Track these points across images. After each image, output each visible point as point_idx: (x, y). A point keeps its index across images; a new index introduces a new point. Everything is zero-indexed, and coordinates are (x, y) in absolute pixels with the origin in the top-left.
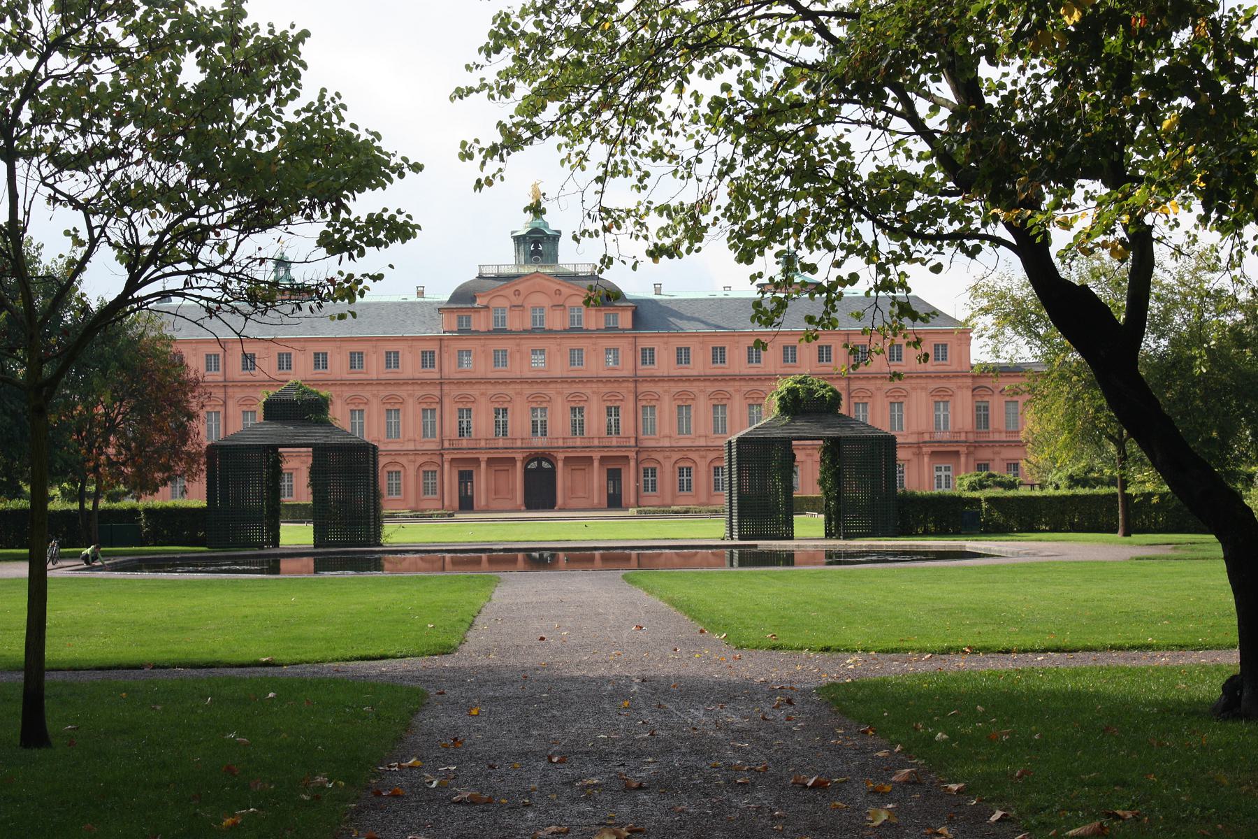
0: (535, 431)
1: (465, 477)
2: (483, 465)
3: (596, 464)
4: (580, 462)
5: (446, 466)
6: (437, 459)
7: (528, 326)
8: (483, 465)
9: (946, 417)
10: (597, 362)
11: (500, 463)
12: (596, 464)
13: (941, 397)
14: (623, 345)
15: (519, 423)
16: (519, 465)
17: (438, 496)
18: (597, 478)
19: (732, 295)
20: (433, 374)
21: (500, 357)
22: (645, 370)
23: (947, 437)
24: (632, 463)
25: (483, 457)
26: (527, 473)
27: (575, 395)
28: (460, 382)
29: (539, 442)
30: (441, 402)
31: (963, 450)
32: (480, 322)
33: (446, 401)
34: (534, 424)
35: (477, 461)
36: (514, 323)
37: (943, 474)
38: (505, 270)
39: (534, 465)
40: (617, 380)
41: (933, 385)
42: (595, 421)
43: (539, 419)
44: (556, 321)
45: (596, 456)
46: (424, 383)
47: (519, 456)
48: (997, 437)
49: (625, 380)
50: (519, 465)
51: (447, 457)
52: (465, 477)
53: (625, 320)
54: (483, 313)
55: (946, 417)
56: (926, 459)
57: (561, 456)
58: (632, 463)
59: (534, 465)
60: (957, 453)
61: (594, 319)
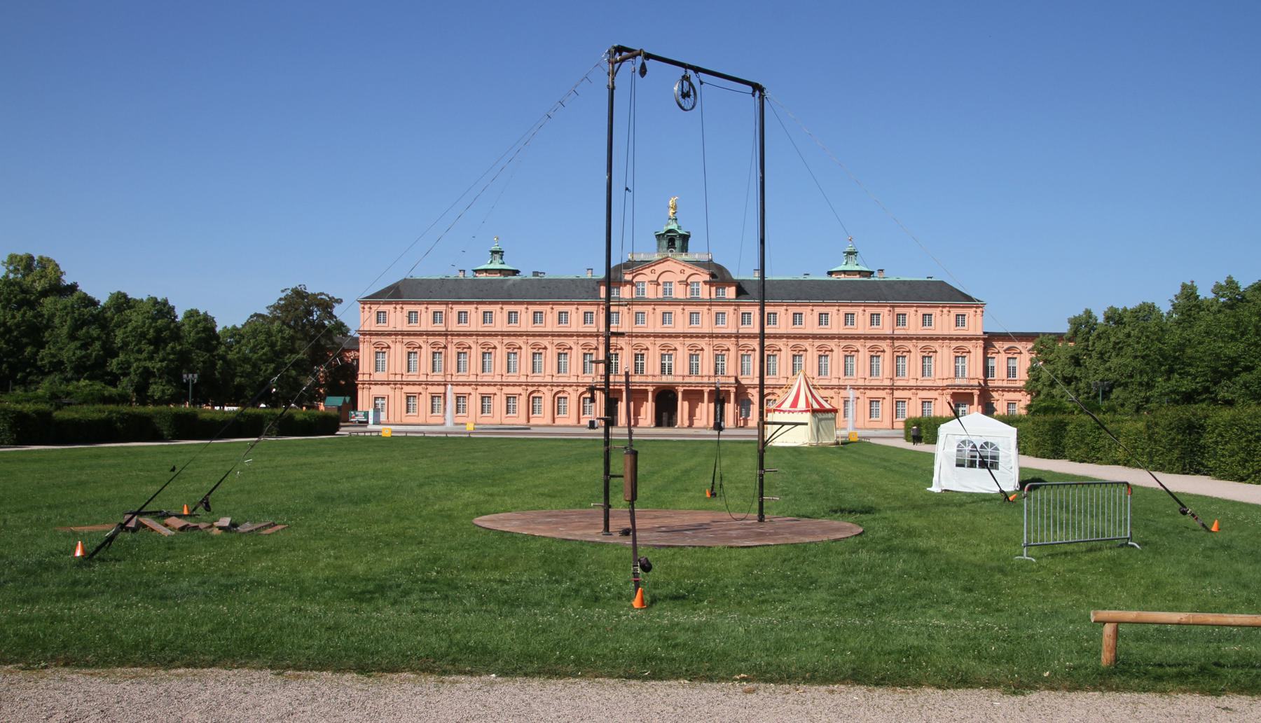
0: (663, 371)
4: (694, 396)
7: (660, 295)
9: (963, 367)
10: (706, 324)
13: (960, 354)
14: (730, 310)
15: (652, 365)
16: (650, 395)
19: (808, 278)
21: (638, 317)
23: (965, 382)
27: (693, 346)
29: (666, 379)
32: (625, 292)
34: (663, 365)
36: (650, 292)
40: (723, 336)
41: (955, 344)
42: (706, 364)
43: (667, 362)
44: (679, 292)
45: (706, 390)
46: (585, 335)
47: (650, 389)
49: (729, 336)
53: (730, 292)
54: (629, 286)
57: (680, 389)
61: (704, 292)
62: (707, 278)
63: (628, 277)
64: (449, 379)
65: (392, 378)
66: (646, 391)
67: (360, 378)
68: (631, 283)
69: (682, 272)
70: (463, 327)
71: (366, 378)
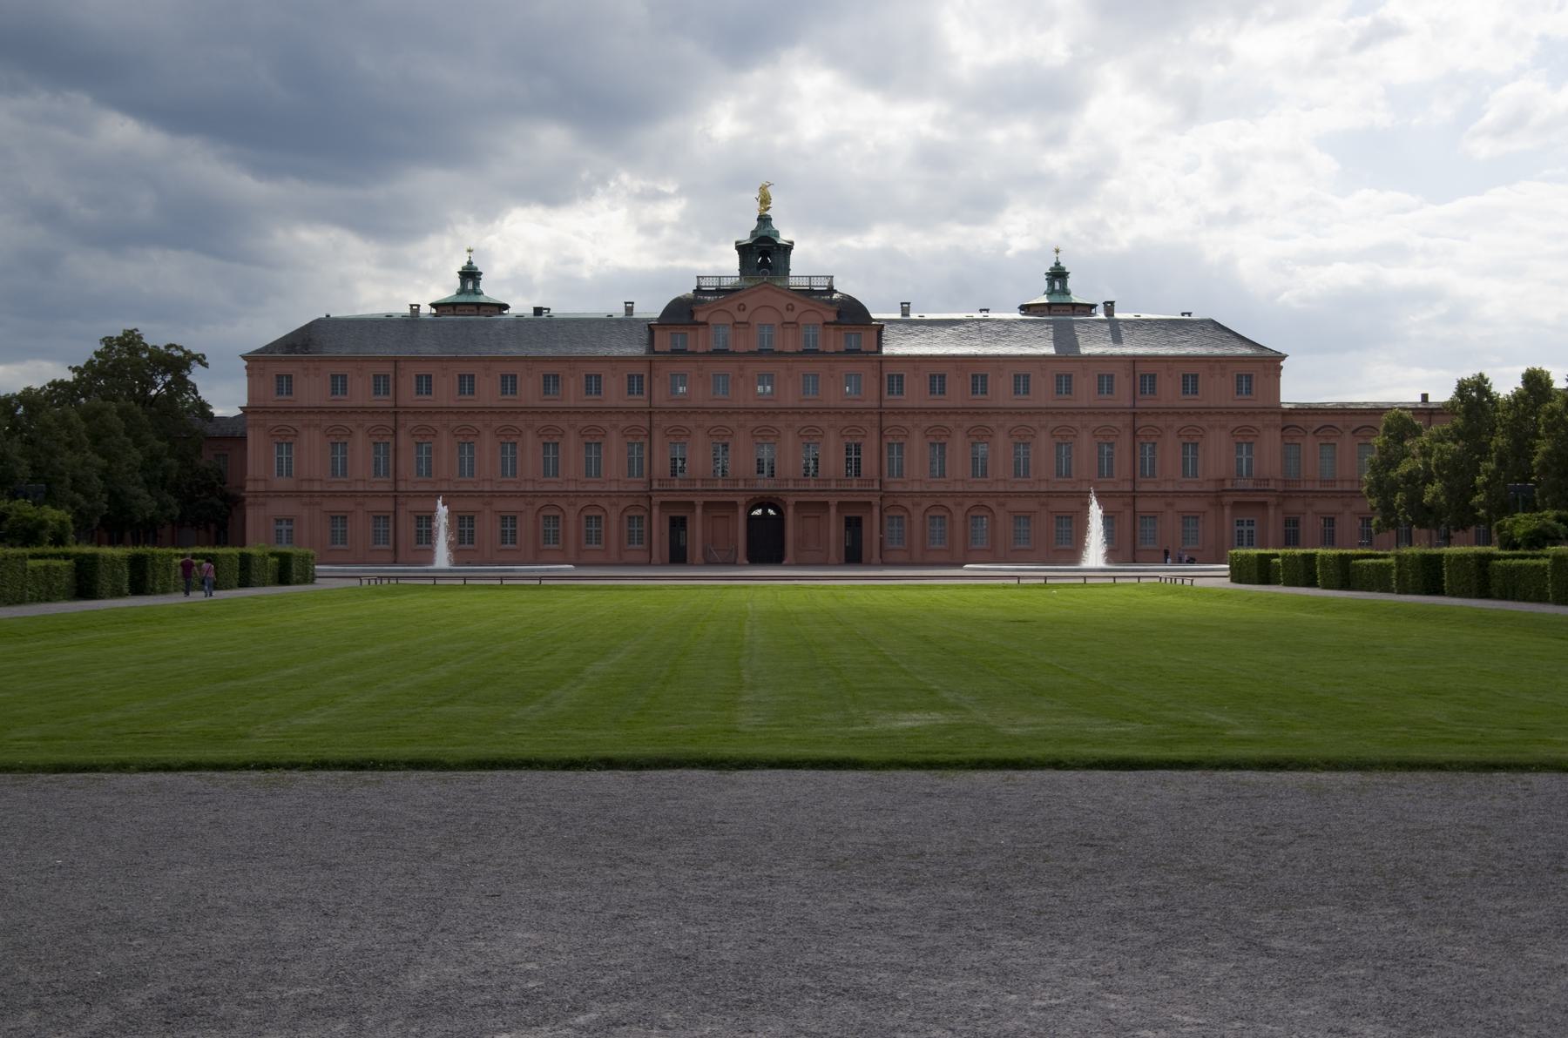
0: (760, 471)
1: (678, 525)
2: (699, 511)
3: (833, 510)
4: (814, 508)
5: (655, 511)
6: (644, 502)
8: (699, 511)
11: (719, 508)
12: (833, 510)
16: (741, 511)
17: (645, 546)
18: (834, 527)
20: (640, 401)
22: (891, 401)
24: (876, 511)
25: (699, 500)
26: (751, 520)
28: (672, 412)
29: (764, 484)
30: (650, 435)
31: (1272, 500)
32: (698, 341)
33: (657, 435)
35: (691, 505)
37: (1245, 528)
38: (726, 283)
39: (758, 512)
40: (858, 412)
42: (833, 460)
46: (629, 412)
47: (741, 500)
48: (1309, 487)
50: (741, 511)
51: (656, 500)
52: (678, 525)
55: (1249, 462)
56: (1227, 511)
57: (791, 500)
58: (876, 511)
59: (758, 512)
60: (1264, 504)
61: (834, 341)
62: (832, 317)
63: (700, 317)
64: (402, 487)
65: (305, 487)
66: (734, 505)
67: (250, 487)
68: (705, 324)
69: (790, 308)
70: (424, 401)
71: (261, 487)
